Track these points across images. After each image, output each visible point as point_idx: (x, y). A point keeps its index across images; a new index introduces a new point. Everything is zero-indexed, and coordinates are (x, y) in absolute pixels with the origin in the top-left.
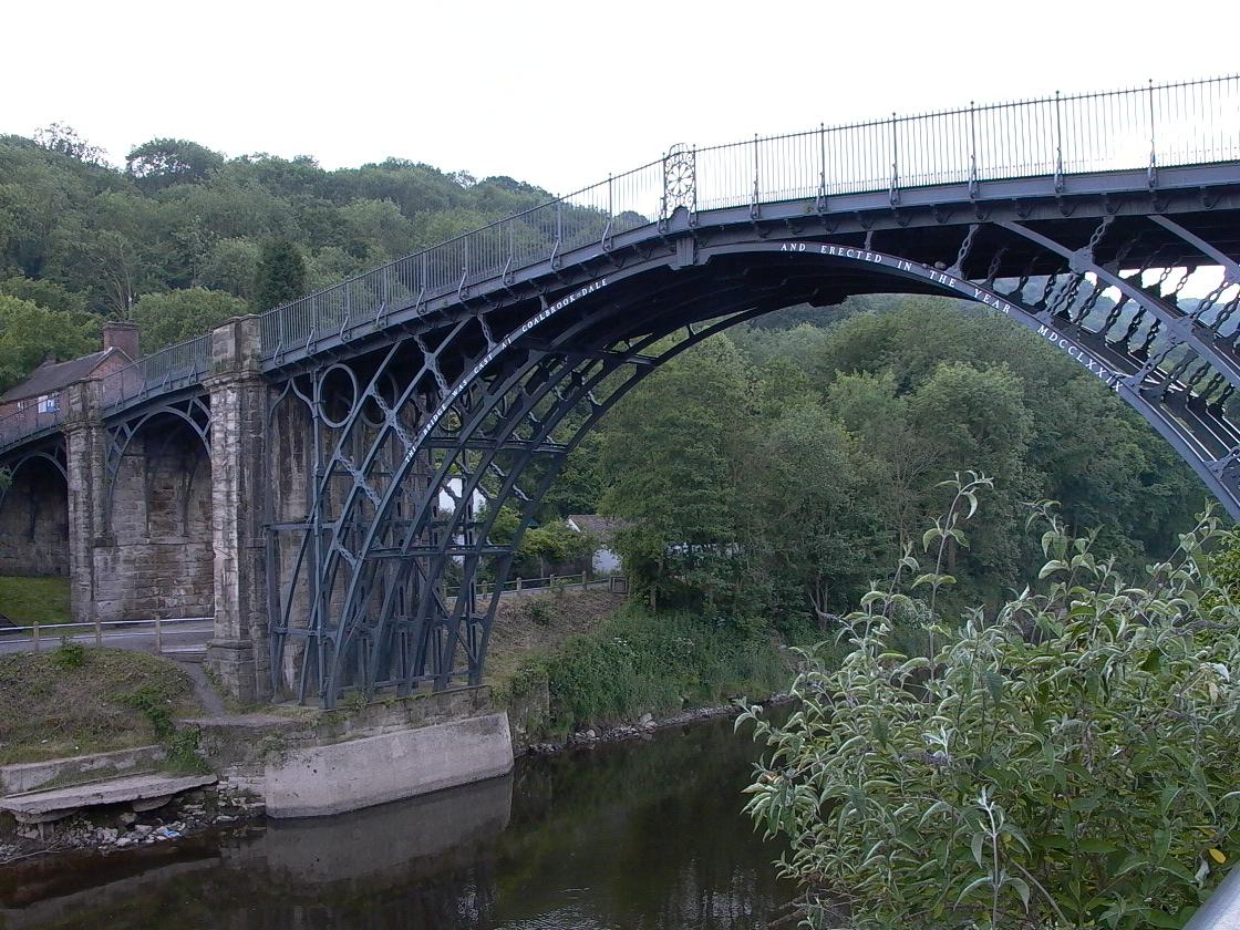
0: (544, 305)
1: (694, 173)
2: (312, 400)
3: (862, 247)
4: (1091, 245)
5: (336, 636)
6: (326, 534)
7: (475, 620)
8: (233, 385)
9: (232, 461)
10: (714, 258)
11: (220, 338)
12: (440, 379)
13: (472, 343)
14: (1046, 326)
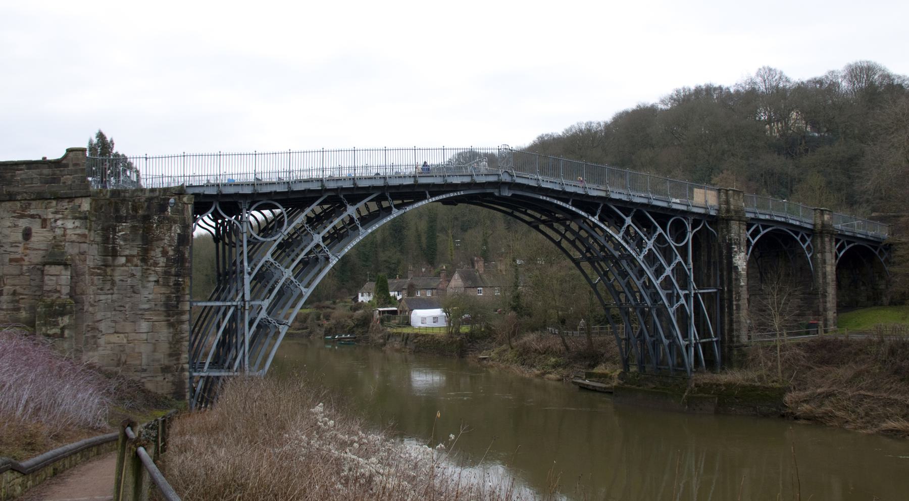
0: (428, 196)
3: (567, 202)
10: (513, 195)
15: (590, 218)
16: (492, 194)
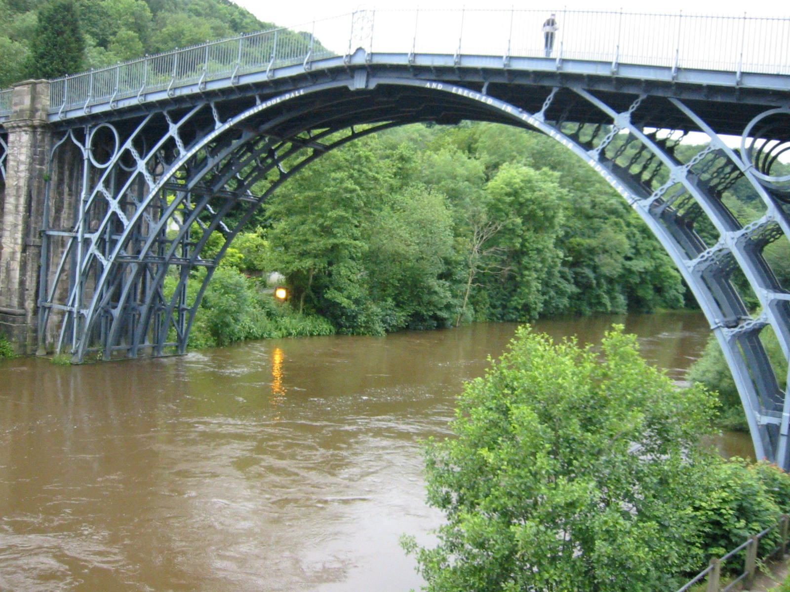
0: (258, 102)
1: (373, 26)
2: (84, 145)
4: (631, 111)
5: (88, 313)
6: (87, 242)
7: (184, 309)
8: (26, 128)
9: (22, 183)
10: (379, 86)
11: (19, 94)
12: (179, 143)
13: (203, 123)
14: (594, 161)
15: (525, 117)
16: (346, 88)
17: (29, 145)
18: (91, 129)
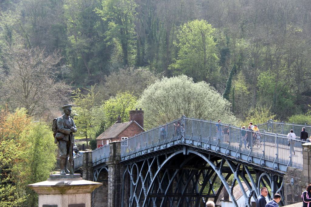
0: (166, 158)
8: (112, 165)
9: (111, 193)
10: (189, 153)
17: (114, 173)
18: (132, 165)
